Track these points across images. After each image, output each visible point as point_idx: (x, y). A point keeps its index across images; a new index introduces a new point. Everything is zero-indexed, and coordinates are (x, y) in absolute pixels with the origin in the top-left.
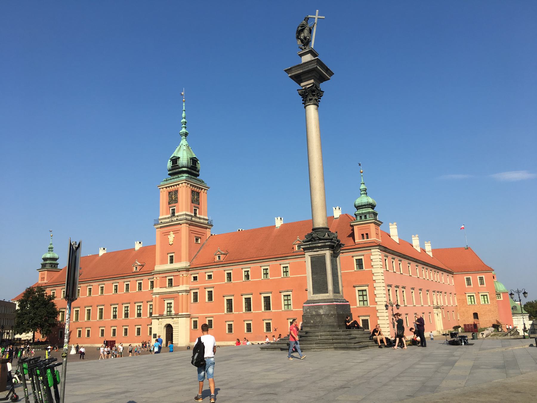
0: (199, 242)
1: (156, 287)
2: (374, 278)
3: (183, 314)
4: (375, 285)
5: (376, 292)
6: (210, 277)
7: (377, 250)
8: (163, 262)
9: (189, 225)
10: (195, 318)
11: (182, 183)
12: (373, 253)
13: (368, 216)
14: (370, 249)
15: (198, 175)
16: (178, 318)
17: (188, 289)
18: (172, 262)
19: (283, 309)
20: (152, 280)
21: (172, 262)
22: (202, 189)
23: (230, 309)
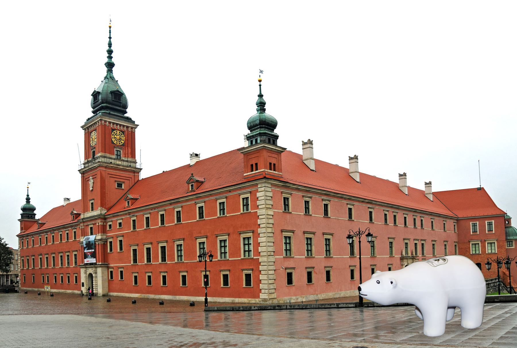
0: (123, 188)
2: (259, 222)
4: (259, 230)
5: (260, 240)
6: (120, 224)
7: (263, 185)
8: (85, 210)
9: (106, 167)
12: (260, 190)
14: (257, 185)
15: (126, 112)
17: (104, 237)
18: (92, 210)
19: (176, 261)
21: (92, 210)
22: (127, 127)
23: (135, 261)
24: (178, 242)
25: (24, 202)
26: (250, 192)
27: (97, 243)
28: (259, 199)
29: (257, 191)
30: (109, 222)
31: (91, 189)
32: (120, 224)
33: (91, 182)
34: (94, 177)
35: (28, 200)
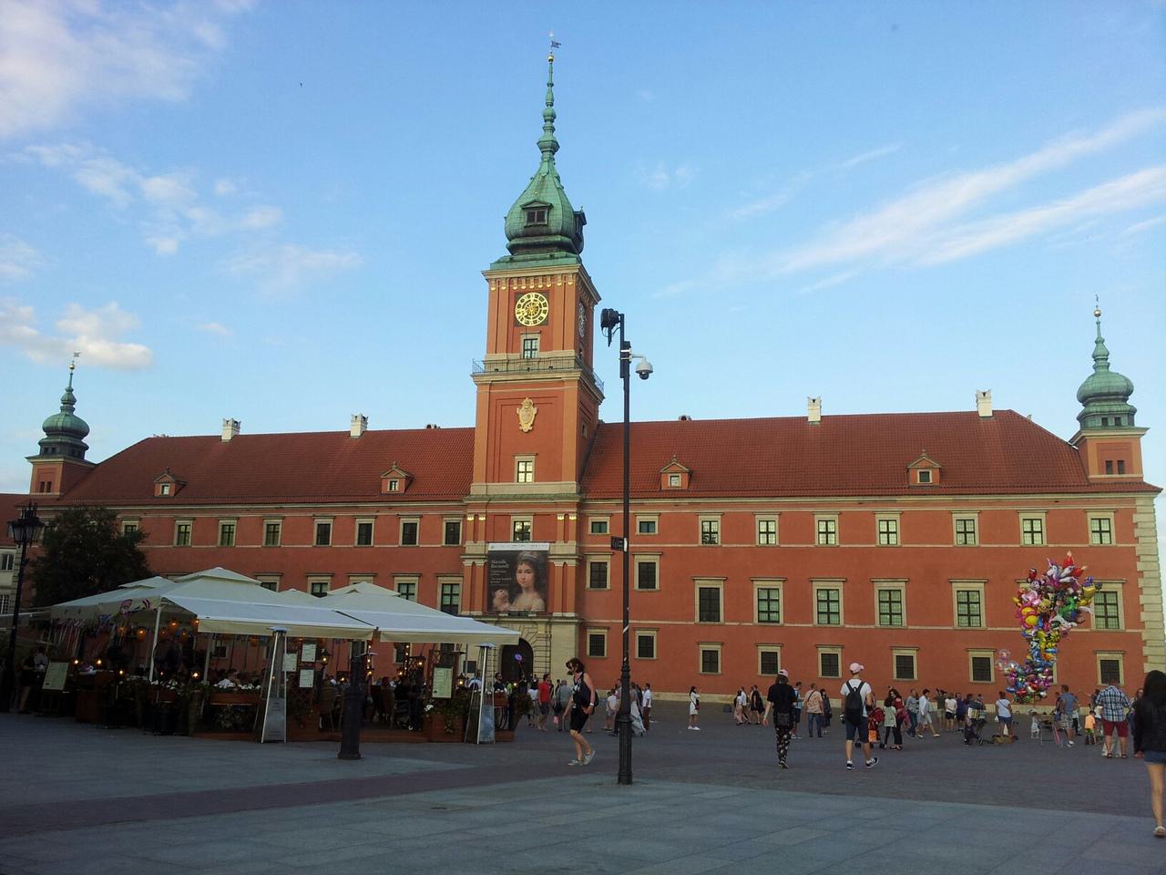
1: (475, 540)
2: (1140, 566)
3: (567, 615)
4: (1141, 583)
5: (1143, 600)
10: (599, 628)
11: (564, 276)
13: (1124, 421)
14: (1134, 500)
16: (550, 624)
20: (454, 520)
24: (885, 584)
25: (55, 408)
26: (1116, 511)
27: (559, 564)
28: (1139, 525)
29: (1135, 511)
30: (602, 515)
31: (526, 427)
32: (647, 526)
33: (526, 417)
34: (542, 401)
35: (69, 402)
